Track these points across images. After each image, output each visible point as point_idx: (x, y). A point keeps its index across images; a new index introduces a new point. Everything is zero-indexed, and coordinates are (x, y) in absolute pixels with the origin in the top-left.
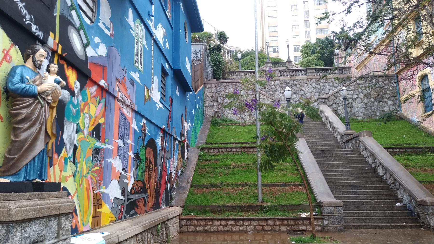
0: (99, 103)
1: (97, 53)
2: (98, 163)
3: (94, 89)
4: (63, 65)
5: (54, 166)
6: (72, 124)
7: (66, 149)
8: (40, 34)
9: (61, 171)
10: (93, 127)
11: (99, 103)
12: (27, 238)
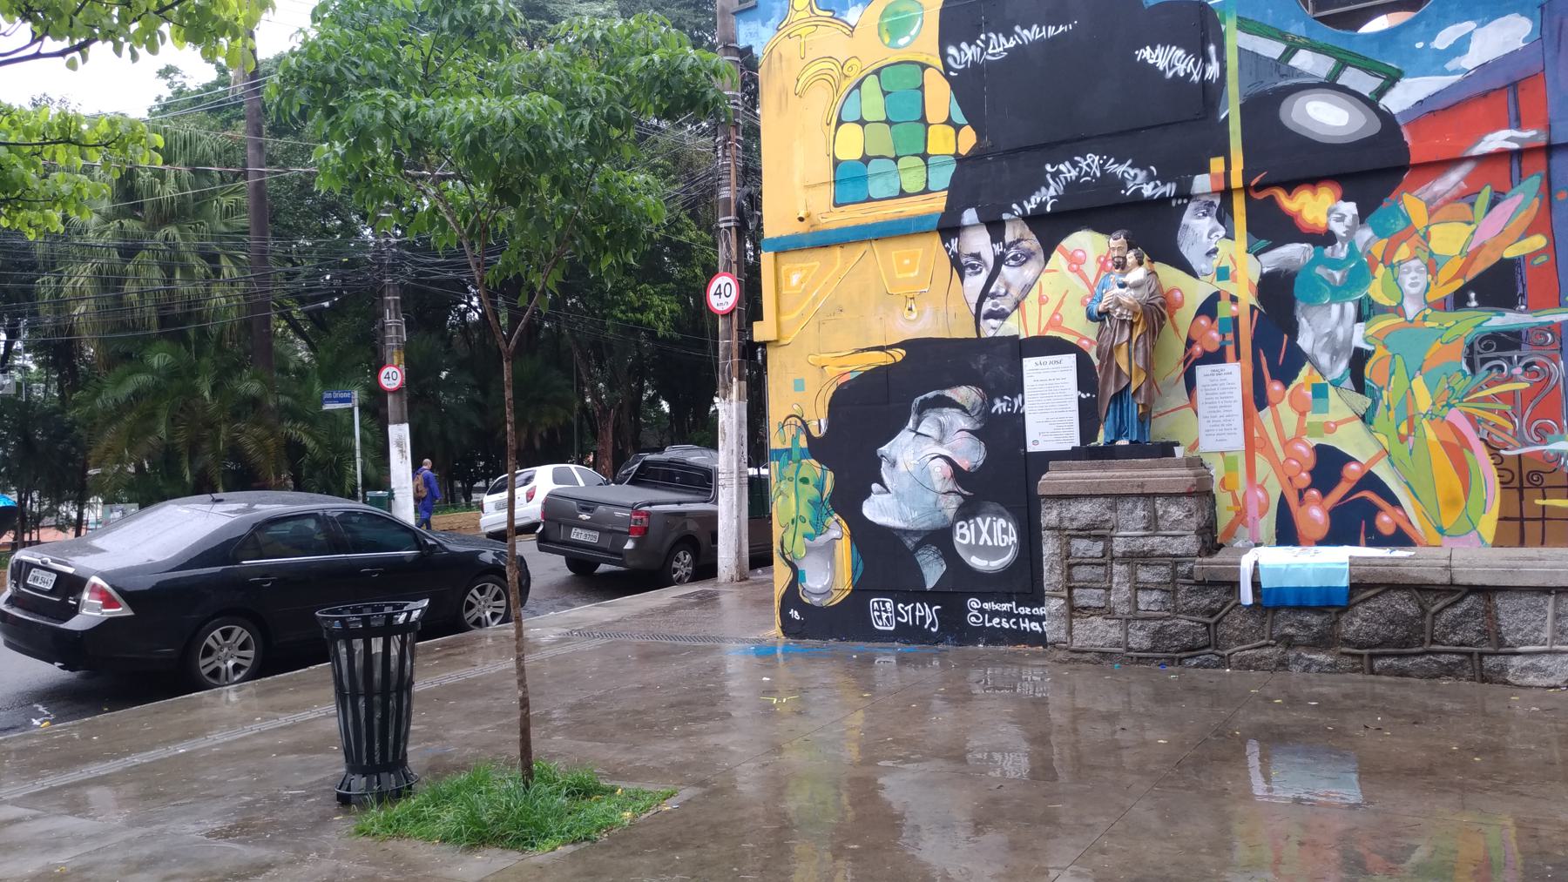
0: (1494, 203)
1: (1455, 72)
2: (1518, 371)
3: (1453, 179)
4: (1272, 200)
5: (1274, 405)
6: (1335, 308)
7: (1316, 366)
8: (1170, 189)
9: (1303, 414)
10: (1459, 283)
11: (1494, 203)
12: (1072, 520)
